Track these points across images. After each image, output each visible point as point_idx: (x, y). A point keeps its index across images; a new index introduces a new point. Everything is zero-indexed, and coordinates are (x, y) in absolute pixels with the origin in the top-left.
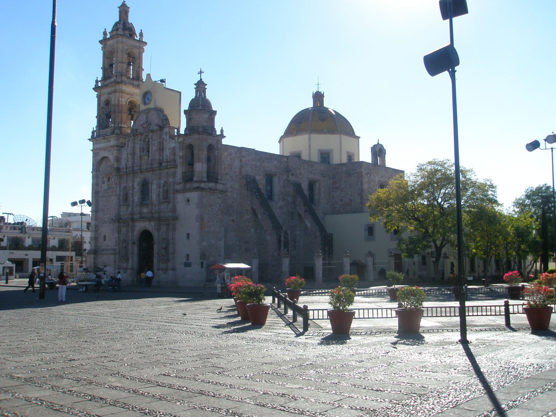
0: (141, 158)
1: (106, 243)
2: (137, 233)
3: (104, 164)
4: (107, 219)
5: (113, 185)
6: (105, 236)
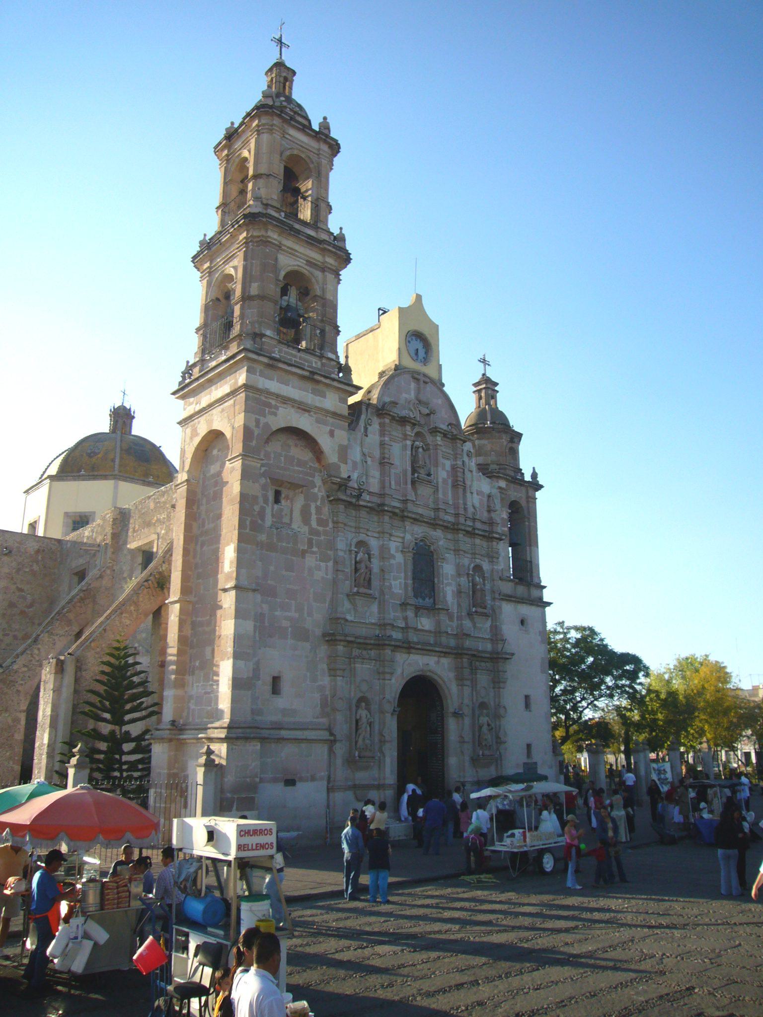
0: (413, 483)
1: (280, 702)
2: (395, 685)
3: (275, 447)
4: (285, 623)
5: (314, 524)
6: (276, 680)
